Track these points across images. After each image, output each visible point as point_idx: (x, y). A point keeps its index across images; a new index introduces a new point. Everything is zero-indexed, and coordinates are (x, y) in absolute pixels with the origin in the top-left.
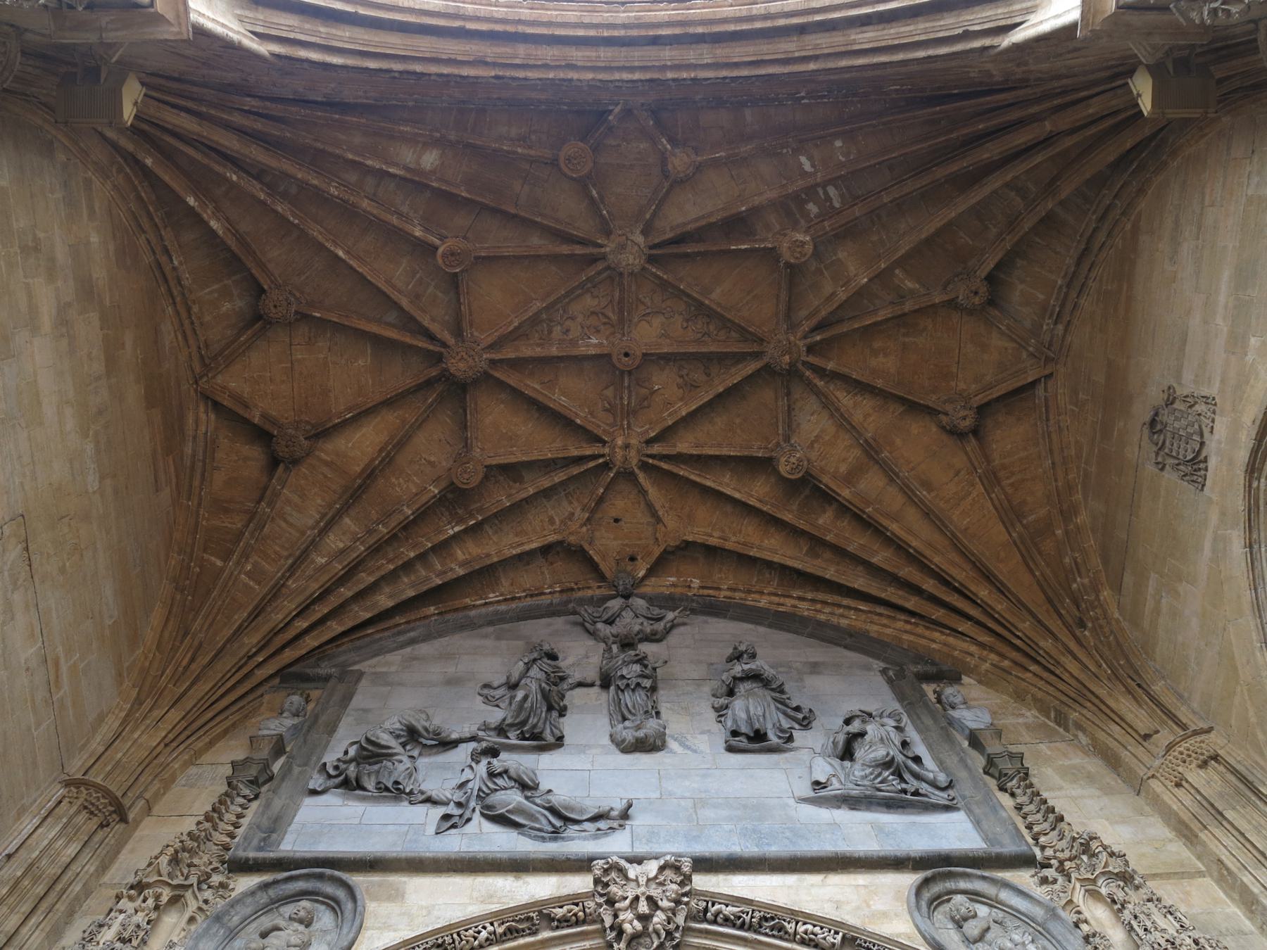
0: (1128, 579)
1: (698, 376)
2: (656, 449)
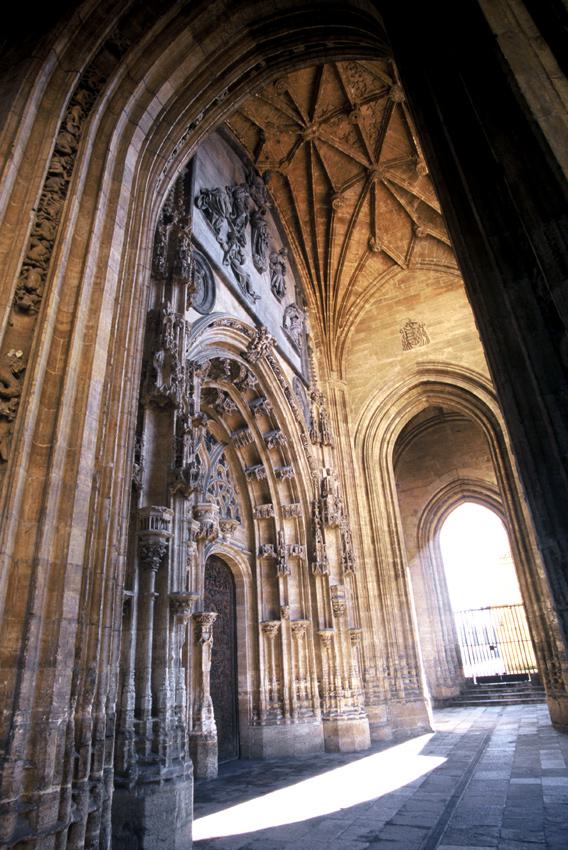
0: (362, 335)
1: (352, 140)
2: (317, 143)
